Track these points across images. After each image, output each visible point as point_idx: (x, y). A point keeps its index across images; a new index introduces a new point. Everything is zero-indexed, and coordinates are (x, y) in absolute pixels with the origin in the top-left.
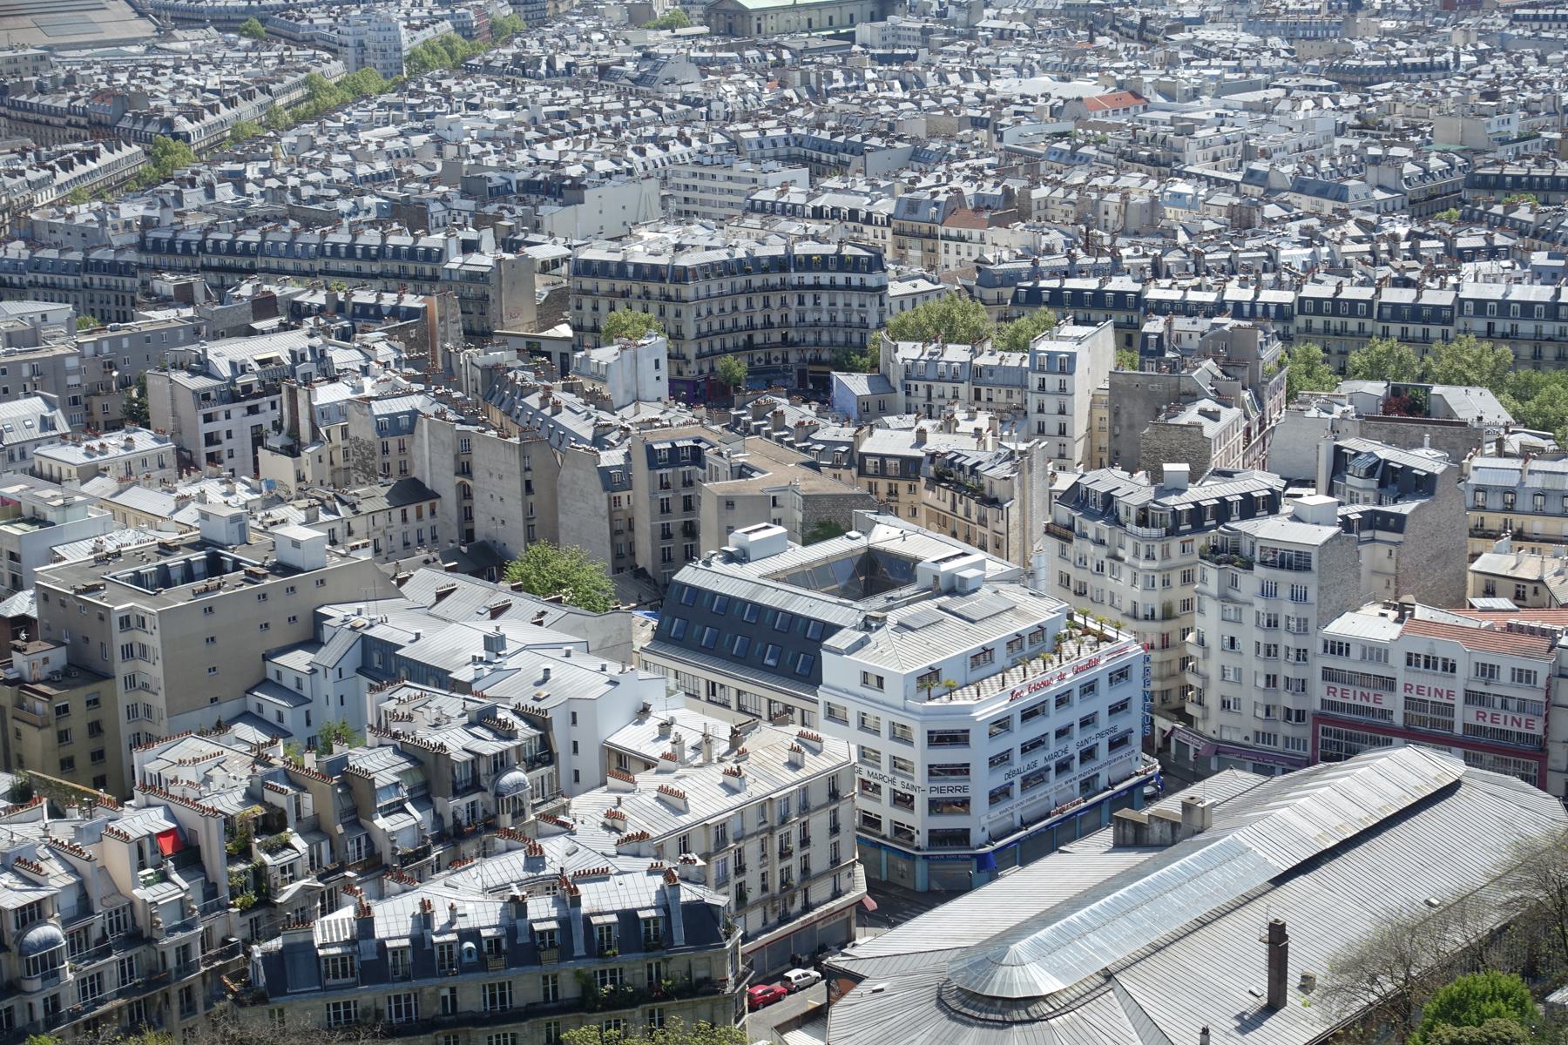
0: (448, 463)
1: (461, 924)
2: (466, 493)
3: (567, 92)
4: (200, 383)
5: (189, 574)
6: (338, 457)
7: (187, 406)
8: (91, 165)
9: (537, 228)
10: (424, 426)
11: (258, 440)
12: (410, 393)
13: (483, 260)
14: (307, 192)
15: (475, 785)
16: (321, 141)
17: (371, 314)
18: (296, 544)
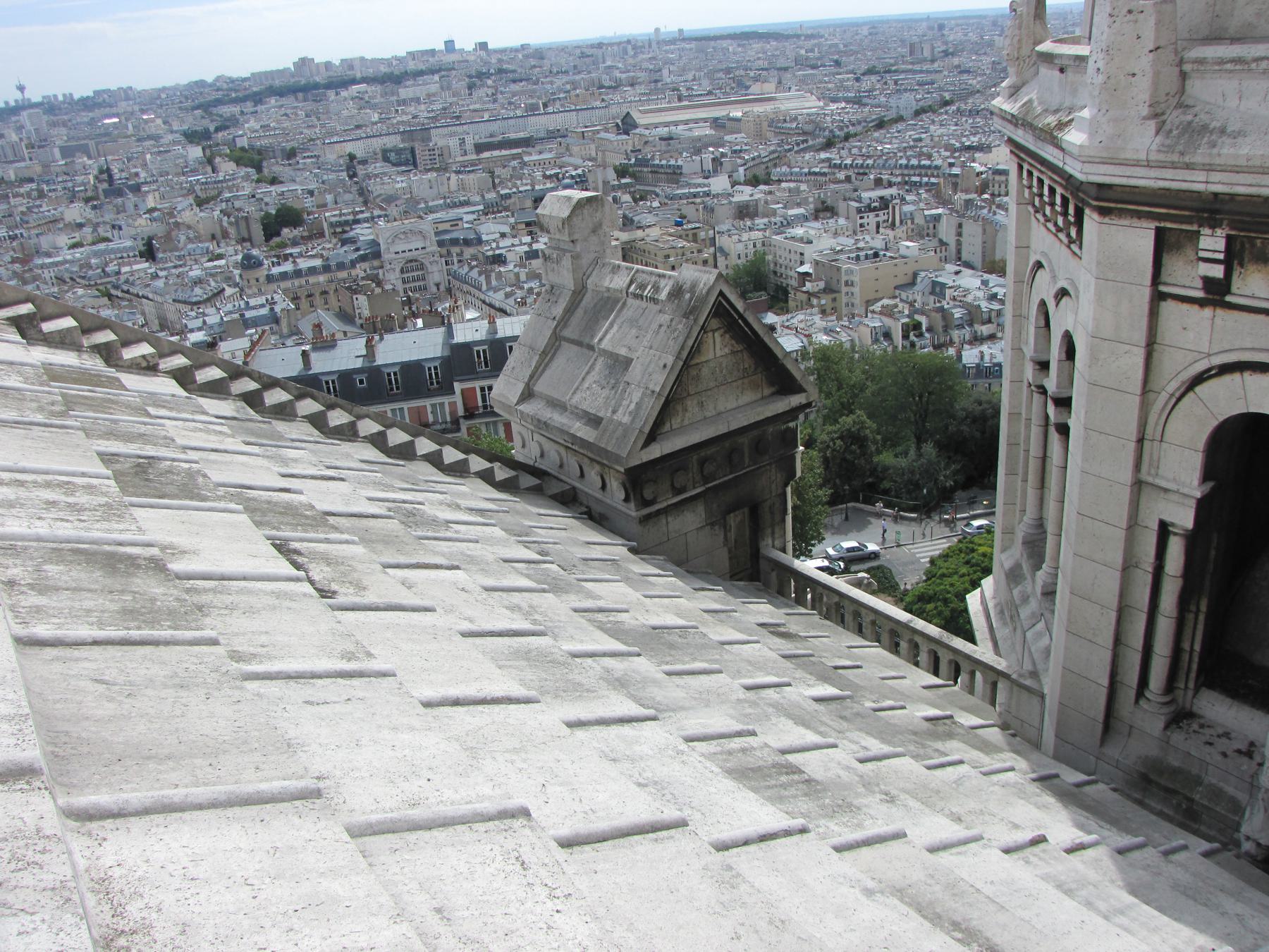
0: (953, 231)
1: (995, 361)
2: (959, 243)
3: (978, 120)
4: (856, 205)
5: (867, 257)
6: (910, 231)
7: (853, 213)
8: (805, 145)
9: (974, 161)
10: (944, 219)
11: (878, 227)
12: (938, 208)
13: (956, 171)
14: (886, 151)
15: (989, 321)
16: (888, 136)
17: (921, 185)
18: (908, 247)
